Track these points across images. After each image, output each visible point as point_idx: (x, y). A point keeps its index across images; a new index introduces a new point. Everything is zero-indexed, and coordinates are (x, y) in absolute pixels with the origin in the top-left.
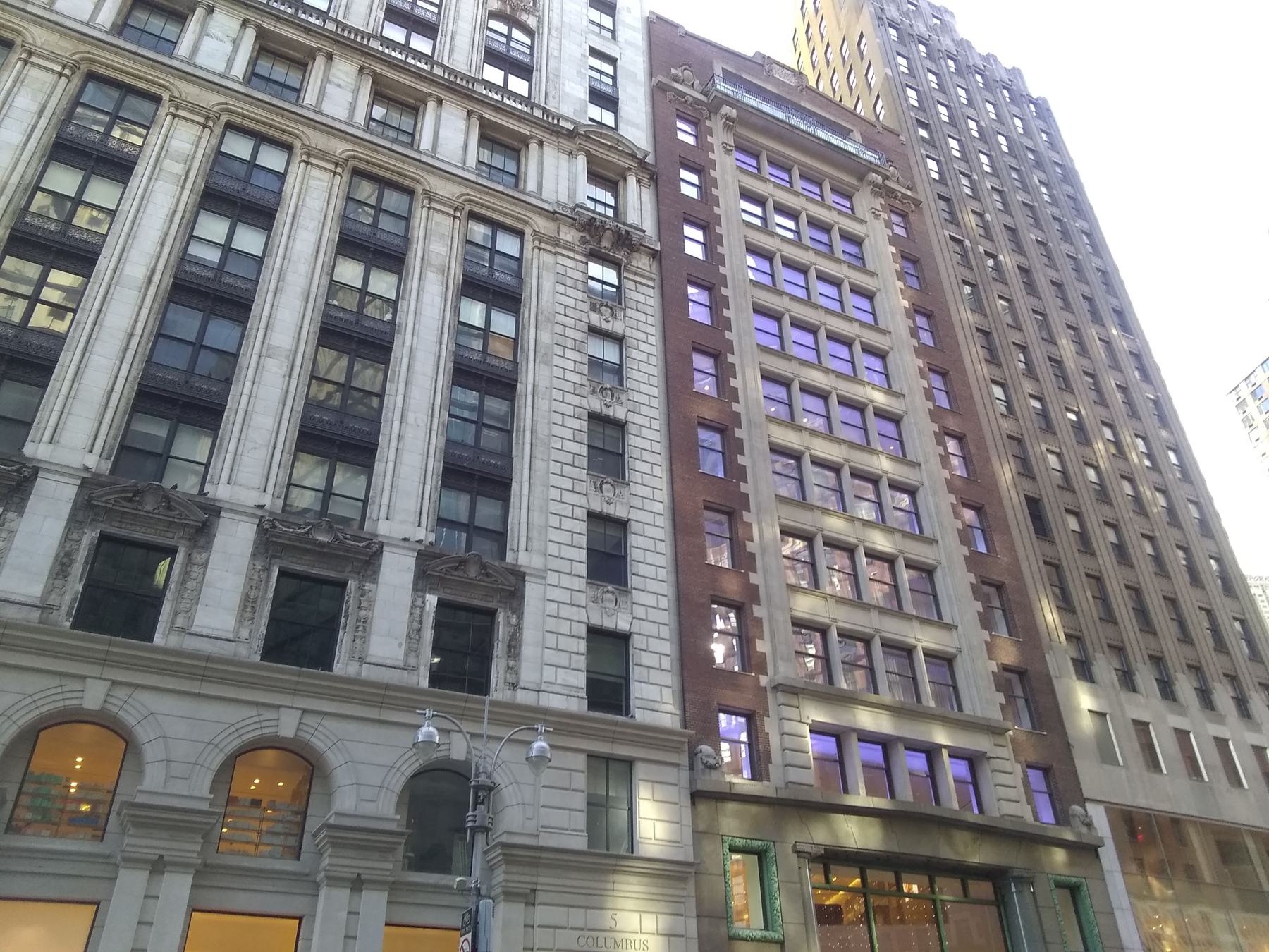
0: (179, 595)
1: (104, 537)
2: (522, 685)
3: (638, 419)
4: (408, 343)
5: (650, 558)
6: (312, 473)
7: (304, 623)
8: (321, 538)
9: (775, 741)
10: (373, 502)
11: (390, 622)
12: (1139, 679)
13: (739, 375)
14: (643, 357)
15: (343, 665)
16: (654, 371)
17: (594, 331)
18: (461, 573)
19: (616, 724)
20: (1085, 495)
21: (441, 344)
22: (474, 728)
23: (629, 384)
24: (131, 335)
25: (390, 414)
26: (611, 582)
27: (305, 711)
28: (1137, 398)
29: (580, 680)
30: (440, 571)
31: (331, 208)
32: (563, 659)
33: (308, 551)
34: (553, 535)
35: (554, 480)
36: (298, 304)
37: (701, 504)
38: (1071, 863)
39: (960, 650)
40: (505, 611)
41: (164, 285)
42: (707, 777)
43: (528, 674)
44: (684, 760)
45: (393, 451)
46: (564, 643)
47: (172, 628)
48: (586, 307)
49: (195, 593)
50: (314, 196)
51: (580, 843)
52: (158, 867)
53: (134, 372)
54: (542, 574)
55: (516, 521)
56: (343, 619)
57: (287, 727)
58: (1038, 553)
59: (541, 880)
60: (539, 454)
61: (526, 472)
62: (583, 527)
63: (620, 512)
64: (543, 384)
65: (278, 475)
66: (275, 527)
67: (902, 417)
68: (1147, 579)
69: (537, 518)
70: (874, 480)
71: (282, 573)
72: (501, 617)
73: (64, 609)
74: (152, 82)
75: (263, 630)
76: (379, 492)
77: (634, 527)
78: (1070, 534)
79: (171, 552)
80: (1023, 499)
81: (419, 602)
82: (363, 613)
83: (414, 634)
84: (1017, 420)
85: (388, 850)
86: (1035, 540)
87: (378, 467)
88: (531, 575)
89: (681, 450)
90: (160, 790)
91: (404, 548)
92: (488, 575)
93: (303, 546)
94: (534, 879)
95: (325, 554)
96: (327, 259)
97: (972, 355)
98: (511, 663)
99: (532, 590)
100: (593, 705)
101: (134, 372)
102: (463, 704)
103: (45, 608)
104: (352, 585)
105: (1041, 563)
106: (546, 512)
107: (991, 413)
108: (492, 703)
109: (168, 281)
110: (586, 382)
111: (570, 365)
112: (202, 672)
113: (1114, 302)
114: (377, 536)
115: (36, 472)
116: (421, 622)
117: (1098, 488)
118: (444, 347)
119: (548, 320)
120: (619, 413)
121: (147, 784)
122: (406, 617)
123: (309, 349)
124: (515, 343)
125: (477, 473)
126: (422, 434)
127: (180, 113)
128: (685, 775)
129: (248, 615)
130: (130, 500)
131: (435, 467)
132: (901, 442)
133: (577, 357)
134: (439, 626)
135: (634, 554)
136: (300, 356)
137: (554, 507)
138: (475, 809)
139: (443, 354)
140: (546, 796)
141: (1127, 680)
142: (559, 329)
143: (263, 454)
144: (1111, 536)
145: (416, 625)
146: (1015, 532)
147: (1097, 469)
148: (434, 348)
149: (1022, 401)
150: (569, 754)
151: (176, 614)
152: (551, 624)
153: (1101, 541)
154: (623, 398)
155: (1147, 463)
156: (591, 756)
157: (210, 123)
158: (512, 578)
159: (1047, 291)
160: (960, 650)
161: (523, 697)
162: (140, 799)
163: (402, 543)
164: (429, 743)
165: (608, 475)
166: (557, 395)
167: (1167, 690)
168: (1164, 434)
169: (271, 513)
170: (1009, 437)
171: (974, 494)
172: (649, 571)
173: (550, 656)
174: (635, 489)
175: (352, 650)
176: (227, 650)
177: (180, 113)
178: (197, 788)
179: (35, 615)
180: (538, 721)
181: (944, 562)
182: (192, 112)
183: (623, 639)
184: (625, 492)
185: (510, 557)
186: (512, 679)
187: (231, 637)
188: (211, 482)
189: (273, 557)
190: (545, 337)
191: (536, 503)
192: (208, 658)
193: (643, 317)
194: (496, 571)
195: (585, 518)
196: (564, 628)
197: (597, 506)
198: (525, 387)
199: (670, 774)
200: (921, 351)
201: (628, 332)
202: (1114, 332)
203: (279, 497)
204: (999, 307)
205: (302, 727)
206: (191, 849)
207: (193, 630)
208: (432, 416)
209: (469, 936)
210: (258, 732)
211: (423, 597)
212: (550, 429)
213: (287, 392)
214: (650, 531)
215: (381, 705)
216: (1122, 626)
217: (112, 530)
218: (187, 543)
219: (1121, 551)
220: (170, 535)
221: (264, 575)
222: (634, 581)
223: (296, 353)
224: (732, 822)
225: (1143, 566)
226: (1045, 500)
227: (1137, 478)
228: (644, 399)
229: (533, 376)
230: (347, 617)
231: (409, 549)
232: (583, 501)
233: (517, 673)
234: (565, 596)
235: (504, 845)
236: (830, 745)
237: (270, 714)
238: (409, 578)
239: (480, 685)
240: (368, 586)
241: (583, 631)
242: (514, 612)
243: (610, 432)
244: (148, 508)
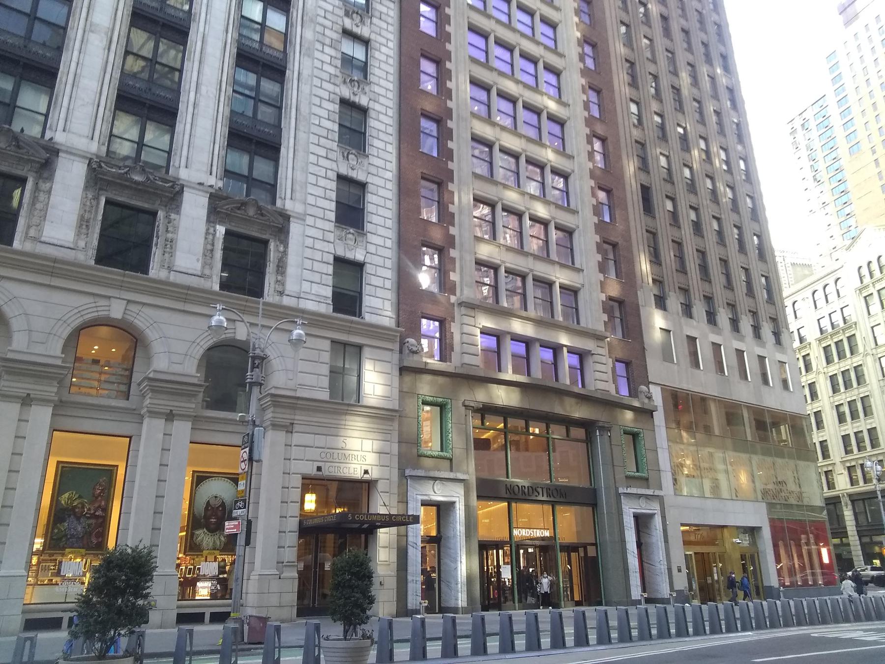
2: (286, 292)
3: (377, 107)
4: (201, 29)
5: (381, 211)
6: (127, 127)
8: (138, 178)
9: (457, 338)
10: (176, 154)
11: (190, 242)
12: (695, 310)
13: (454, 79)
14: (383, 58)
15: (156, 271)
16: (391, 70)
17: (347, 33)
18: (243, 212)
19: (352, 322)
20: (681, 186)
22: (253, 320)
23: (372, 78)
25: (187, 87)
26: (352, 226)
27: (129, 301)
28: (726, 121)
29: (328, 292)
30: (227, 209)
32: (316, 278)
33: (127, 187)
34: (311, 189)
35: (313, 148)
37: (420, 175)
38: (635, 420)
39: (583, 285)
40: (275, 241)
42: (411, 358)
43: (291, 286)
44: (397, 347)
46: (317, 266)
47: (27, 237)
48: (341, 13)
49: (43, 213)
51: (325, 395)
52: (26, 401)
54: (302, 217)
55: (284, 176)
56: (155, 239)
57: (116, 311)
58: (643, 224)
59: (297, 417)
60: (301, 127)
62: (333, 185)
63: (361, 176)
64: (306, 73)
65: (102, 128)
66: (101, 167)
67: (566, 122)
68: (711, 246)
69: (299, 176)
70: (541, 166)
71: (108, 202)
72: (272, 246)
75: (95, 243)
76: (180, 147)
77: (370, 188)
78: (667, 213)
79: (22, 181)
80: (639, 186)
81: (211, 230)
82: (170, 235)
83: (209, 253)
84: (643, 130)
85: (191, 395)
86: (642, 215)
87: (179, 127)
88: (294, 217)
89: (408, 134)
90: (25, 351)
91: (199, 190)
92: (262, 215)
93: (123, 183)
94: (292, 417)
95: (140, 190)
97: (620, 79)
98: (279, 278)
99: (295, 228)
100: (335, 310)
102: (245, 303)
104: (161, 214)
105: (644, 231)
106: (306, 172)
107: (627, 123)
108: (265, 304)
110: (339, 74)
111: (328, 59)
113: (722, 49)
114: (179, 179)
116: (213, 245)
117: (689, 182)
118: (230, 35)
119: (312, 21)
120: (363, 101)
121: (15, 345)
122: (202, 241)
124: (286, 37)
125: (254, 138)
126: (212, 104)
128: (396, 356)
129: (84, 231)
131: (222, 131)
132: (563, 140)
133: (333, 52)
134: (225, 249)
135: (369, 208)
137: (312, 169)
138: (252, 371)
139: (229, 41)
140: (302, 366)
141: (688, 310)
142: (319, 29)
143: (90, 110)
144: (693, 216)
145: (209, 247)
146: (630, 210)
147: (691, 169)
148: (221, 35)
149: (649, 115)
150: (318, 340)
151: (29, 227)
152: (308, 253)
153: (685, 219)
154: (367, 89)
155: (725, 167)
156: (334, 342)
158: (281, 219)
159: (678, 35)
160: (583, 285)
161: (287, 301)
162: (10, 356)
163: (198, 186)
164: (219, 327)
165: (353, 148)
166: (317, 82)
167: (711, 317)
168: (739, 148)
169: (97, 156)
170: (637, 142)
171: (608, 181)
172: (380, 221)
173: (307, 275)
174: (372, 160)
175: (163, 261)
176: (69, 255)
178: (52, 350)
180: (297, 317)
181: (581, 227)
183: (359, 266)
184: (365, 162)
185: (279, 203)
186: (280, 289)
187: (72, 246)
188: (51, 128)
189: (100, 189)
190: (309, 35)
191: (299, 164)
192: (55, 260)
193: (384, 25)
195: (335, 178)
196: (318, 256)
197: (344, 171)
198: (292, 73)
199: (387, 355)
200: (585, 72)
201: (373, 37)
202: (719, 71)
203: (103, 144)
204: (643, 45)
205: (127, 312)
206: (50, 390)
207: (43, 239)
209: (247, 450)
210: (96, 314)
211: (214, 227)
212: (310, 109)
213: (107, 62)
214: (382, 192)
215: (185, 301)
216: (689, 275)
218: (35, 175)
219: (697, 227)
220: (21, 167)
222: (368, 227)
224: (426, 387)
225: (710, 237)
226: (654, 188)
227: (716, 177)
228: (382, 91)
229: (299, 66)
230: (158, 237)
231: (203, 191)
233: (283, 284)
235: (273, 395)
236: (492, 342)
237: (102, 302)
238: (203, 213)
239: (257, 291)
240: (173, 216)
241: (331, 259)
242: (281, 243)
243: (356, 115)
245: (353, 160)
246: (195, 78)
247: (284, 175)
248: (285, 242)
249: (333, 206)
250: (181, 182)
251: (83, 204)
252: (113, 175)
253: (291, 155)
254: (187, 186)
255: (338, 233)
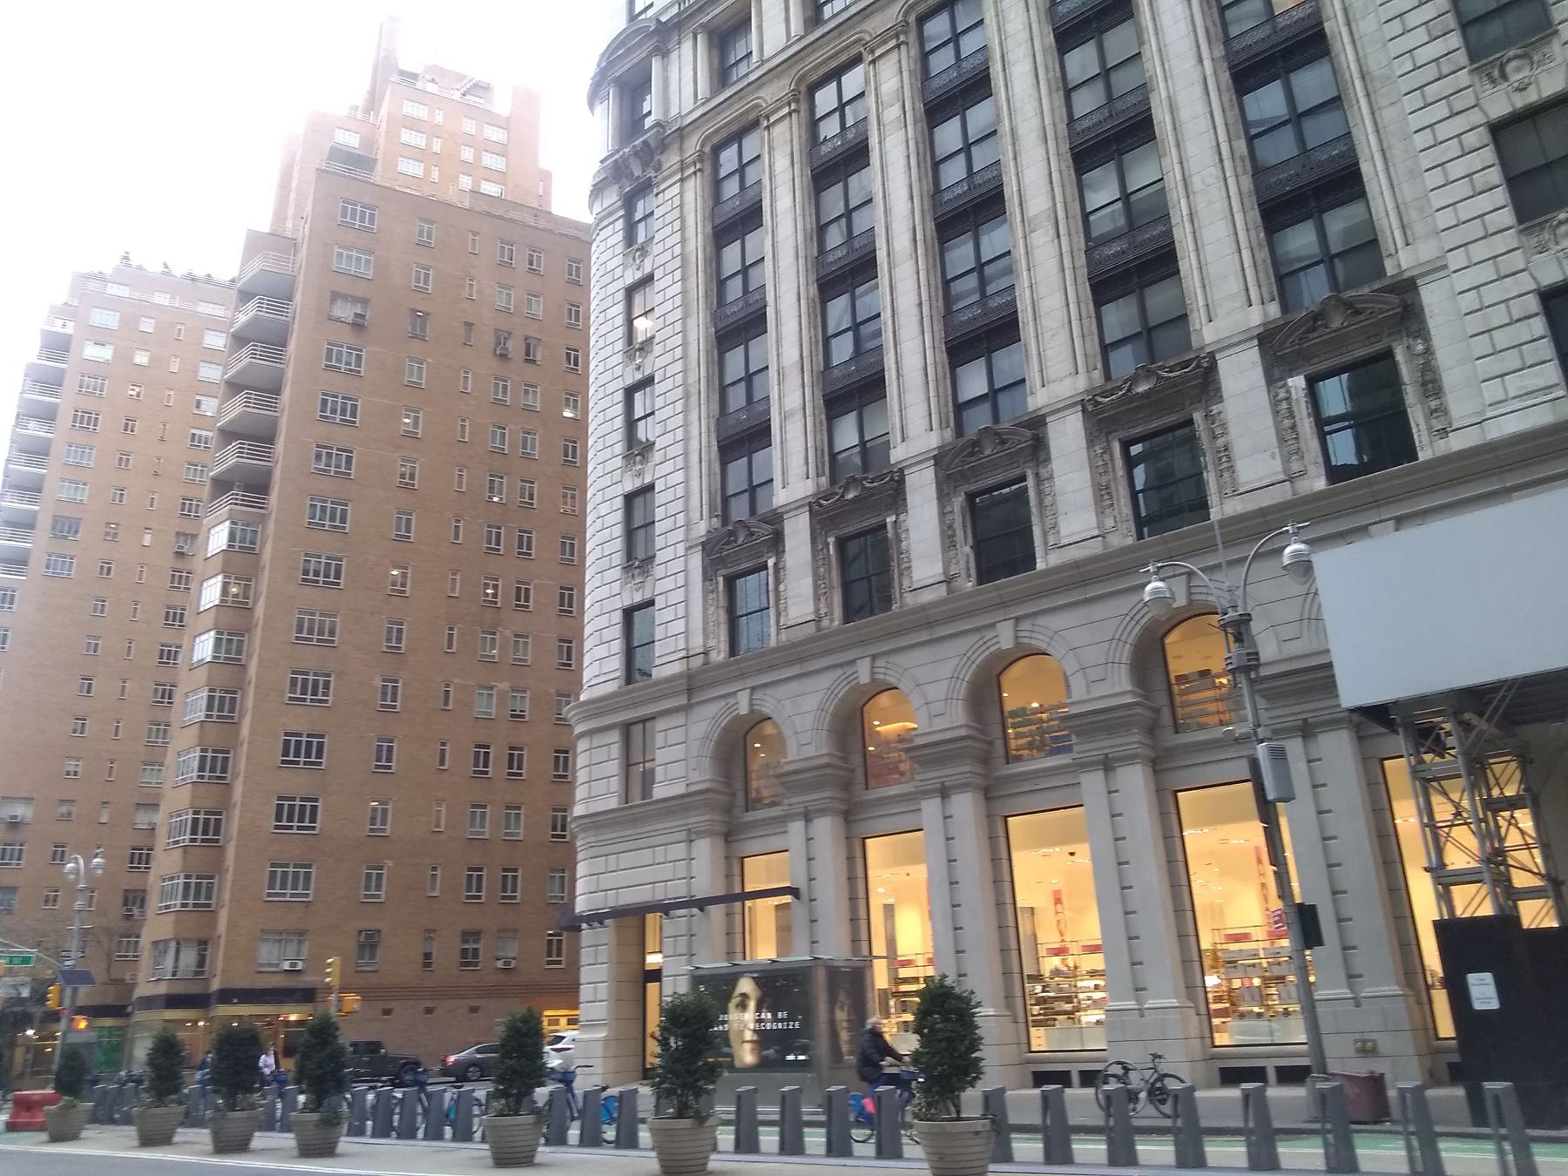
0: (1042, 516)
1: (971, 497)
7: (999, 537)
15: (1221, 509)
18: (1322, 331)
21: (1201, 61)
24: (920, 304)
31: (1033, 12)
32: (1511, 360)
34: (1438, 199)
36: (1039, 152)
41: (929, 235)
43: (1460, 406)
45: (1190, 237)
46: (1502, 339)
50: (1012, 16)
53: (937, 335)
54: (1440, 263)
61: (1373, 139)
69: (1408, 191)
72: (1400, 355)
73: (963, 573)
74: (847, 47)
75: (1126, 510)
79: (1023, 478)
81: (1282, 394)
82: (1220, 442)
90: (1085, 697)
96: (1051, 74)
98: (1433, 404)
99: (1432, 297)
101: (937, 335)
103: (949, 580)
104: (1198, 417)
108: (1224, 523)
109: (931, 226)
112: (1090, 578)
115: (901, 470)
118: (1207, 63)
122: (1269, 420)
123: (1068, 190)
125: (1306, 188)
126: (1217, 192)
127: (878, 53)
130: (972, 454)
136: (1060, 207)
143: (1063, 336)
145: (1287, 423)
148: (1195, 75)
157: (902, 38)
158: (1393, 298)
161: (1457, 442)
176: (1095, 548)
177: (878, 53)
178: (1118, 686)
179: (944, 587)
182: (885, 42)
187: (1096, 533)
189: (1108, 433)
194: (1366, 301)
197: (1500, 104)
207: (1064, 541)
208: (1221, 160)
211: (1285, 385)
217: (973, 487)
221: (1106, 457)
223: (1055, 205)
232: (1476, 117)
233: (1446, 412)
234: (1488, 272)
238: (1257, 375)
239: (1407, 451)
240: (1215, 409)
241: (1533, 303)
244: (987, 452)
245: (1518, 70)
246: (1179, 177)
247: (1382, 209)
248: (1423, 333)
249: (1501, 196)
250: (1208, 350)
251: (1093, 467)
252: (1112, 405)
253: (1380, 166)
254: (1219, 350)
255: (1534, 241)
